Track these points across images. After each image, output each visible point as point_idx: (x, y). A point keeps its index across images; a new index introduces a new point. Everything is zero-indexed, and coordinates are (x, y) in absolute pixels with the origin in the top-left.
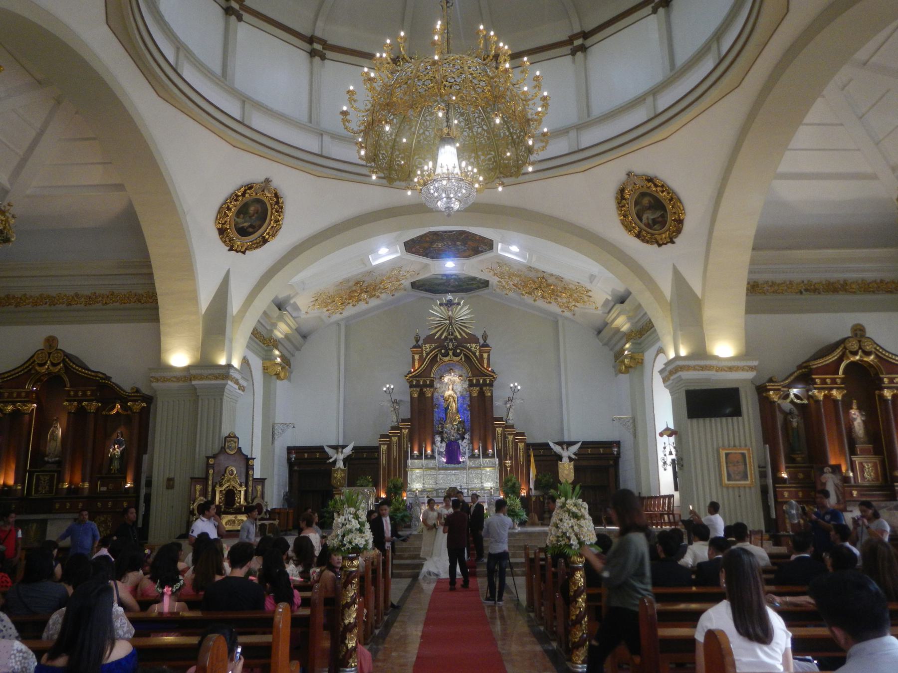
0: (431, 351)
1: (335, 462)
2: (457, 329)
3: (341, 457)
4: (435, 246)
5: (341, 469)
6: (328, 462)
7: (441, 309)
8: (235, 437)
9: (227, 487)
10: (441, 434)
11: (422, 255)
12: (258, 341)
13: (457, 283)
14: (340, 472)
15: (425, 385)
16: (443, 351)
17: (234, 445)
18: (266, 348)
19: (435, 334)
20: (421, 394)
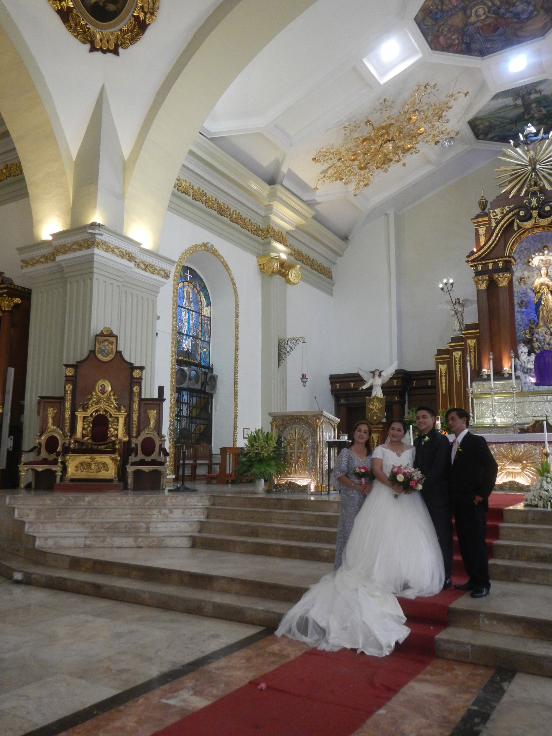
0: (503, 218)
1: (371, 388)
2: (544, 176)
3: (378, 382)
4: (473, 19)
5: (378, 398)
6: (360, 389)
7: (517, 152)
8: (111, 335)
9: (96, 411)
10: (529, 342)
11: (461, 52)
12: (249, 234)
13: (544, 112)
15: (497, 270)
16: (522, 213)
17: (108, 347)
18: (262, 241)
19: (509, 192)
20: (492, 284)
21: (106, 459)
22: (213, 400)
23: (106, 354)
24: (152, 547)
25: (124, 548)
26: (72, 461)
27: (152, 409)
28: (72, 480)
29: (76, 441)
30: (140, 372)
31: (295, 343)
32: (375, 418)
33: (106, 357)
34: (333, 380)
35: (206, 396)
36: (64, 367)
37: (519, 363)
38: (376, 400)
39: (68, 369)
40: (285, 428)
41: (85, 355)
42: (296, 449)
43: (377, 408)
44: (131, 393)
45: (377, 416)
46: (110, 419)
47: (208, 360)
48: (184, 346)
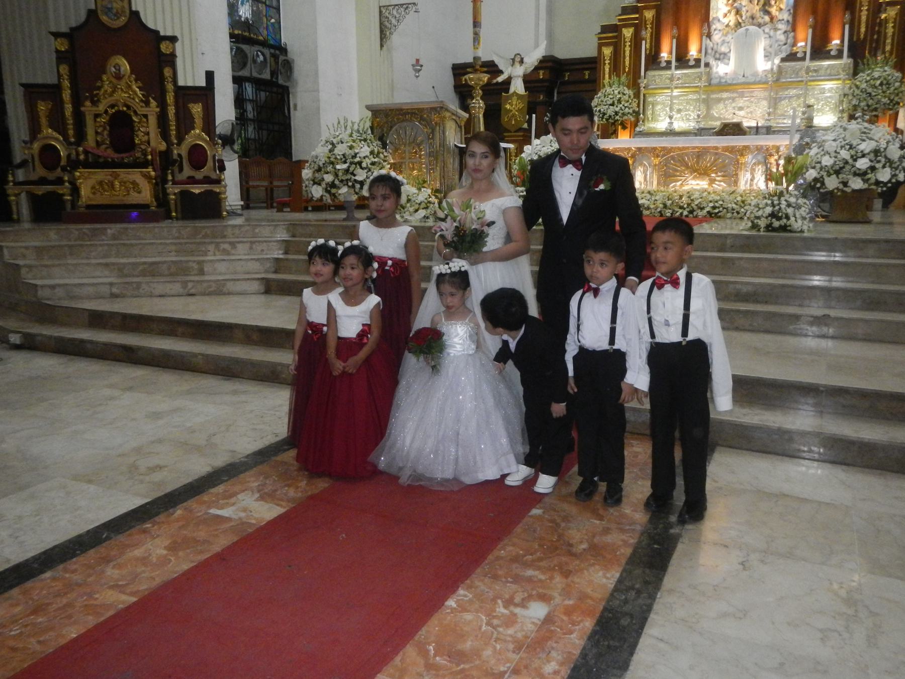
3: (519, 71)
5: (517, 95)
6: (495, 81)
9: (112, 106)
14: (515, 100)
21: (135, 175)
22: (291, 96)
23: (115, 15)
24: (210, 294)
25: (169, 296)
26: (86, 179)
27: (195, 102)
28: (88, 207)
29: (86, 152)
30: (171, 45)
31: (403, 13)
32: (513, 122)
33: (115, 20)
34: (457, 72)
35: (280, 90)
36: (52, 38)
37: (710, 44)
38: (515, 98)
39: (59, 40)
40: (391, 127)
41: (83, 17)
42: (407, 158)
43: (517, 109)
44: (162, 78)
45: (516, 120)
46: (135, 119)
47: (278, 37)
48: (241, 13)
